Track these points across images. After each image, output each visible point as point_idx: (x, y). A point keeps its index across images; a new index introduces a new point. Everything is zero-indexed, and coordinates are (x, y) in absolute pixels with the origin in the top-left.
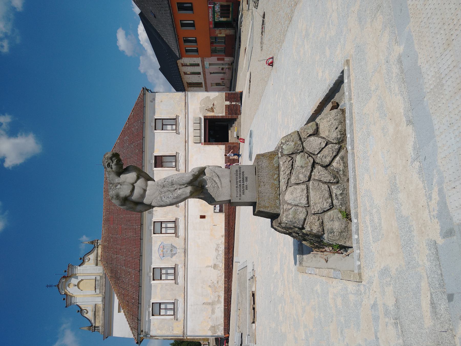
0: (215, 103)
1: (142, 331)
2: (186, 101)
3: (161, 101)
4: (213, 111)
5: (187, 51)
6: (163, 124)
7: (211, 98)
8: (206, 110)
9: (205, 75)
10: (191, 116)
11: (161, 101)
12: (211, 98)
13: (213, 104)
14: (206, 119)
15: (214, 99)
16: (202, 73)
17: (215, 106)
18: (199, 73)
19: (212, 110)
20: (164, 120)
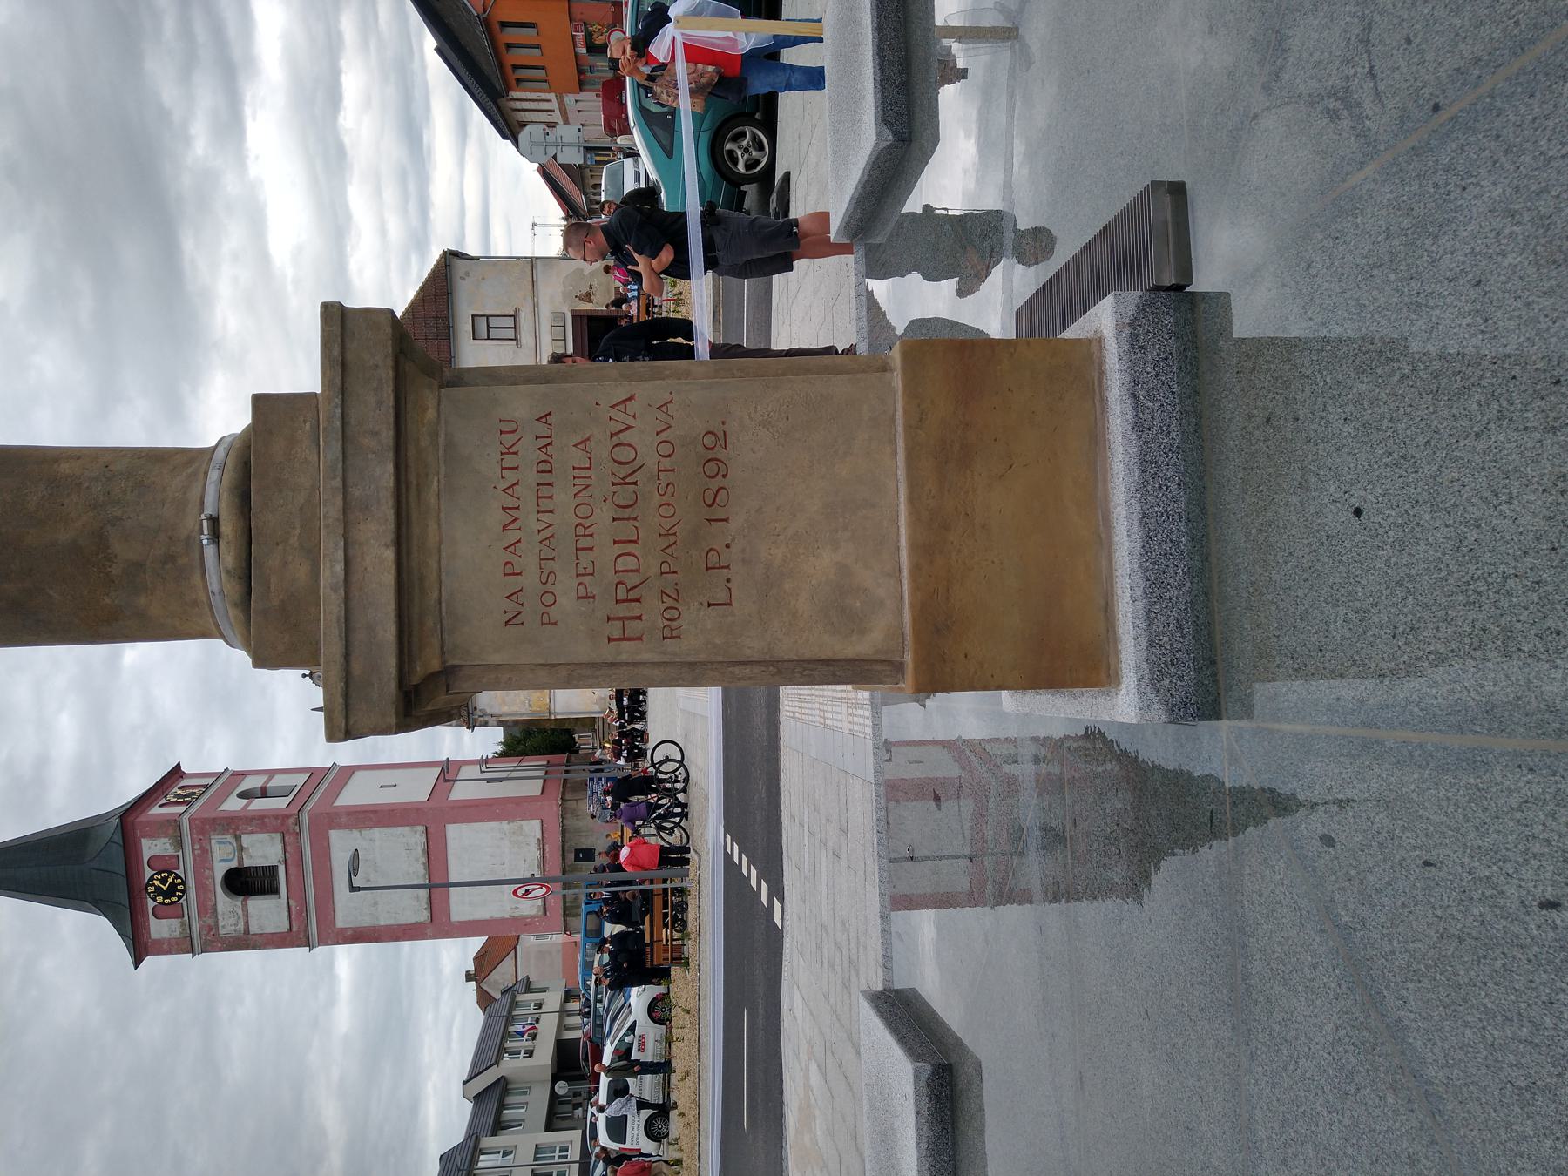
0: (595, 284)
1: (476, 709)
2: (535, 279)
3: (483, 279)
4: (590, 301)
5: (518, 81)
6: (488, 325)
7: (586, 273)
8: (576, 297)
9: (566, 113)
10: (545, 311)
11: (483, 279)
12: (586, 273)
13: (591, 285)
14: (578, 317)
15: (592, 274)
16: (557, 112)
17: (594, 290)
18: (553, 111)
19: (588, 297)
20: (490, 318)
